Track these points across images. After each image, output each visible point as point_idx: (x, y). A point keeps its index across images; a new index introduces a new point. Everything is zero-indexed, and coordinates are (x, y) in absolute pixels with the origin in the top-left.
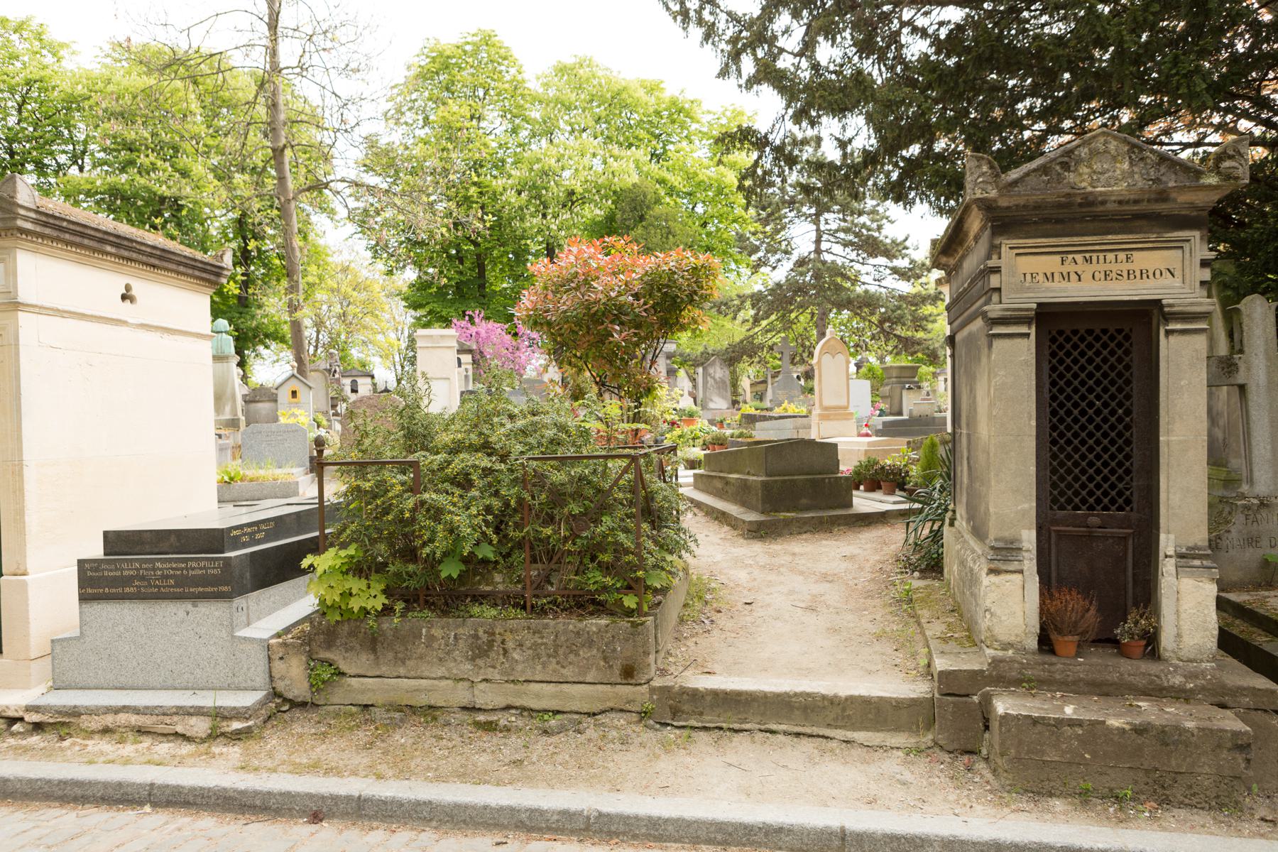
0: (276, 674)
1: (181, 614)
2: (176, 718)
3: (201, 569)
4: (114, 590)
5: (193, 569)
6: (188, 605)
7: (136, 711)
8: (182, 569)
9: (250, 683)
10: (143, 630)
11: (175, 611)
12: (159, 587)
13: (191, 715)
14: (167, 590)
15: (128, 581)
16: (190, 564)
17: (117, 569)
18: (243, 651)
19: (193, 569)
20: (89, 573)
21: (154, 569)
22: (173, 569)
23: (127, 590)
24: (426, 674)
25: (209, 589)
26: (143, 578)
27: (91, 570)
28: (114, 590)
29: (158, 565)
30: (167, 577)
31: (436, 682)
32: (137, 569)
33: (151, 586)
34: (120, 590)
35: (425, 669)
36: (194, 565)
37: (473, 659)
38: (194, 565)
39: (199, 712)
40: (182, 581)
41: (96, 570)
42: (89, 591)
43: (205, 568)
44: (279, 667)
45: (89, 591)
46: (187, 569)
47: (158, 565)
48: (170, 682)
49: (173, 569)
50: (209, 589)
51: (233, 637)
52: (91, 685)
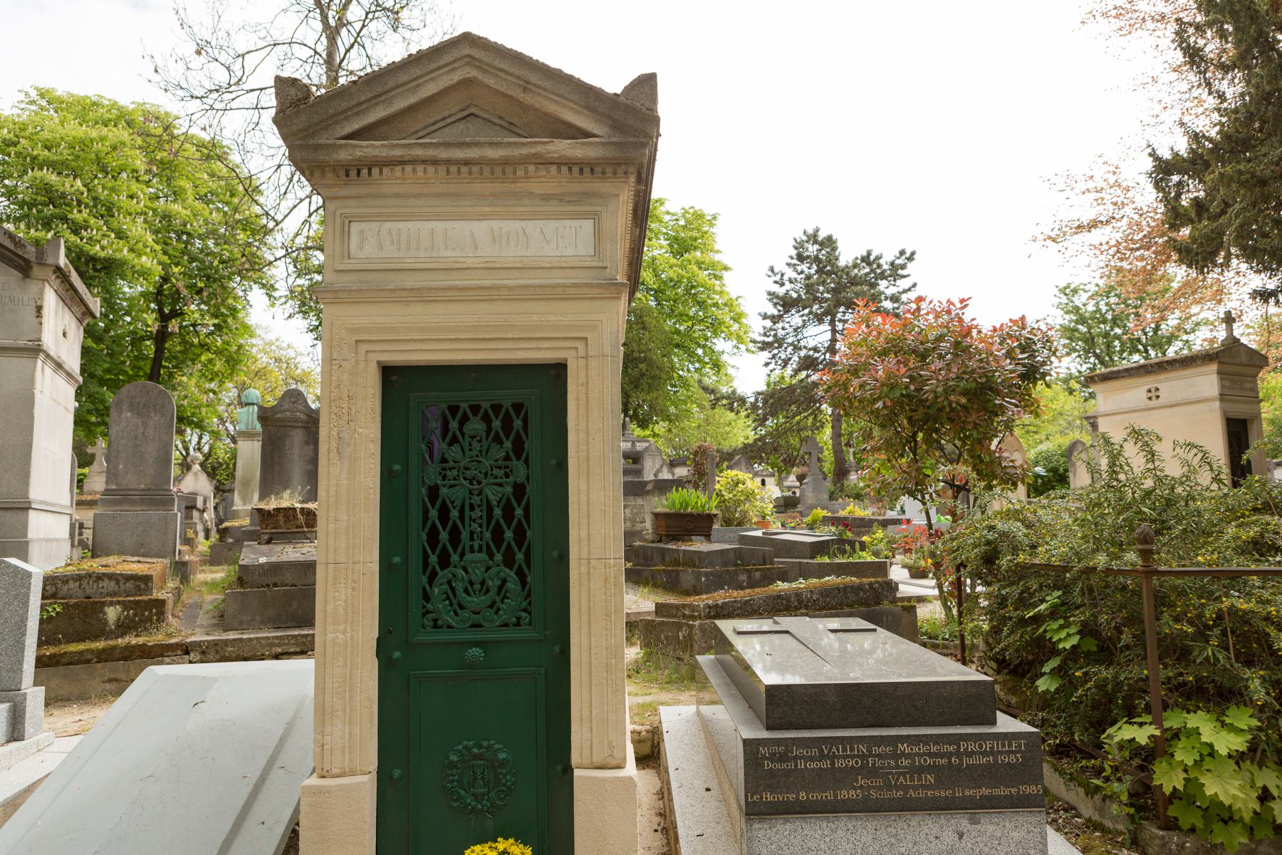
1: (949, 837)
3: (985, 754)
4: (816, 796)
5: (970, 754)
6: (963, 822)
8: (949, 755)
11: (935, 831)
12: (906, 788)
14: (921, 794)
17: (822, 757)
19: (970, 754)
20: (768, 765)
21: (896, 756)
22: (931, 755)
23: (844, 794)
25: (1002, 791)
26: (873, 772)
27: (772, 758)
29: (904, 747)
30: (921, 770)
32: (863, 757)
33: (889, 786)
36: (972, 747)
38: (972, 747)
41: (783, 758)
42: (768, 797)
43: (992, 752)
45: (768, 797)
47: (904, 747)
49: (931, 755)
50: (1002, 791)
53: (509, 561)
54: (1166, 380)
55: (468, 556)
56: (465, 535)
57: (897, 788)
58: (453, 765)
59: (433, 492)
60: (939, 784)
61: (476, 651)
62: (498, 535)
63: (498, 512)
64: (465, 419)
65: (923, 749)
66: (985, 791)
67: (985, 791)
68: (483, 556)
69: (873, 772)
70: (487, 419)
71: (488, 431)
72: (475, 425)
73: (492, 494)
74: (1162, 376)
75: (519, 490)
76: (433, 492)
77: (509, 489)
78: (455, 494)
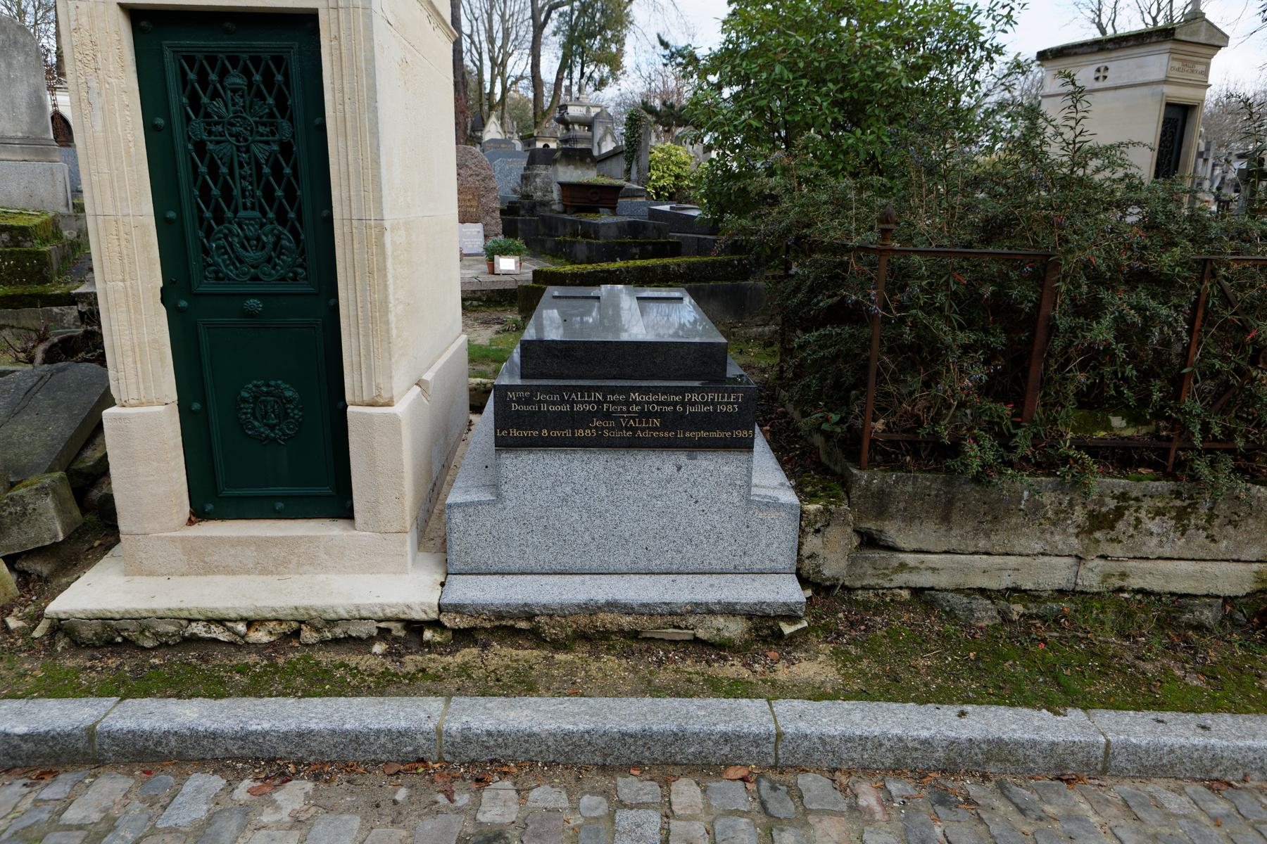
0: (806, 551)
1: (669, 468)
2: (692, 620)
3: (706, 404)
4: (557, 433)
5: (693, 404)
6: (682, 458)
7: (627, 609)
8: (675, 404)
9: (768, 565)
10: (603, 491)
11: (658, 464)
12: (634, 430)
13: (711, 612)
14: (647, 434)
15: (582, 420)
16: (687, 397)
17: (563, 402)
18: (762, 521)
19: (693, 404)
21: (628, 403)
22: (658, 403)
24: (1017, 549)
25: (718, 434)
26: (608, 416)
27: (519, 401)
28: (557, 433)
29: (635, 396)
31: (1028, 560)
32: (598, 403)
33: (621, 429)
34: (568, 433)
35: (1020, 544)
36: (695, 397)
37: (1091, 532)
38: (695, 397)
39: (730, 610)
40: (674, 421)
41: (528, 401)
42: (515, 433)
43: (712, 403)
44: (813, 543)
46: (683, 403)
47: (635, 396)
48: (642, 565)
49: (658, 403)
50: (718, 434)
51: (749, 502)
52: (514, 568)
53: (282, 218)
54: (1118, 58)
55: (242, 213)
56: (236, 192)
57: (627, 429)
58: (245, 400)
59: (200, 147)
60: (664, 428)
61: (253, 303)
62: (268, 192)
63: (266, 170)
64: (223, 73)
65: (652, 398)
66: (703, 434)
67: (703, 434)
68: (257, 214)
69: (608, 416)
70: (247, 73)
71: (250, 85)
72: (236, 79)
73: (260, 152)
74: (1114, 54)
75: (286, 149)
76: (200, 147)
77: (275, 148)
78: (222, 150)
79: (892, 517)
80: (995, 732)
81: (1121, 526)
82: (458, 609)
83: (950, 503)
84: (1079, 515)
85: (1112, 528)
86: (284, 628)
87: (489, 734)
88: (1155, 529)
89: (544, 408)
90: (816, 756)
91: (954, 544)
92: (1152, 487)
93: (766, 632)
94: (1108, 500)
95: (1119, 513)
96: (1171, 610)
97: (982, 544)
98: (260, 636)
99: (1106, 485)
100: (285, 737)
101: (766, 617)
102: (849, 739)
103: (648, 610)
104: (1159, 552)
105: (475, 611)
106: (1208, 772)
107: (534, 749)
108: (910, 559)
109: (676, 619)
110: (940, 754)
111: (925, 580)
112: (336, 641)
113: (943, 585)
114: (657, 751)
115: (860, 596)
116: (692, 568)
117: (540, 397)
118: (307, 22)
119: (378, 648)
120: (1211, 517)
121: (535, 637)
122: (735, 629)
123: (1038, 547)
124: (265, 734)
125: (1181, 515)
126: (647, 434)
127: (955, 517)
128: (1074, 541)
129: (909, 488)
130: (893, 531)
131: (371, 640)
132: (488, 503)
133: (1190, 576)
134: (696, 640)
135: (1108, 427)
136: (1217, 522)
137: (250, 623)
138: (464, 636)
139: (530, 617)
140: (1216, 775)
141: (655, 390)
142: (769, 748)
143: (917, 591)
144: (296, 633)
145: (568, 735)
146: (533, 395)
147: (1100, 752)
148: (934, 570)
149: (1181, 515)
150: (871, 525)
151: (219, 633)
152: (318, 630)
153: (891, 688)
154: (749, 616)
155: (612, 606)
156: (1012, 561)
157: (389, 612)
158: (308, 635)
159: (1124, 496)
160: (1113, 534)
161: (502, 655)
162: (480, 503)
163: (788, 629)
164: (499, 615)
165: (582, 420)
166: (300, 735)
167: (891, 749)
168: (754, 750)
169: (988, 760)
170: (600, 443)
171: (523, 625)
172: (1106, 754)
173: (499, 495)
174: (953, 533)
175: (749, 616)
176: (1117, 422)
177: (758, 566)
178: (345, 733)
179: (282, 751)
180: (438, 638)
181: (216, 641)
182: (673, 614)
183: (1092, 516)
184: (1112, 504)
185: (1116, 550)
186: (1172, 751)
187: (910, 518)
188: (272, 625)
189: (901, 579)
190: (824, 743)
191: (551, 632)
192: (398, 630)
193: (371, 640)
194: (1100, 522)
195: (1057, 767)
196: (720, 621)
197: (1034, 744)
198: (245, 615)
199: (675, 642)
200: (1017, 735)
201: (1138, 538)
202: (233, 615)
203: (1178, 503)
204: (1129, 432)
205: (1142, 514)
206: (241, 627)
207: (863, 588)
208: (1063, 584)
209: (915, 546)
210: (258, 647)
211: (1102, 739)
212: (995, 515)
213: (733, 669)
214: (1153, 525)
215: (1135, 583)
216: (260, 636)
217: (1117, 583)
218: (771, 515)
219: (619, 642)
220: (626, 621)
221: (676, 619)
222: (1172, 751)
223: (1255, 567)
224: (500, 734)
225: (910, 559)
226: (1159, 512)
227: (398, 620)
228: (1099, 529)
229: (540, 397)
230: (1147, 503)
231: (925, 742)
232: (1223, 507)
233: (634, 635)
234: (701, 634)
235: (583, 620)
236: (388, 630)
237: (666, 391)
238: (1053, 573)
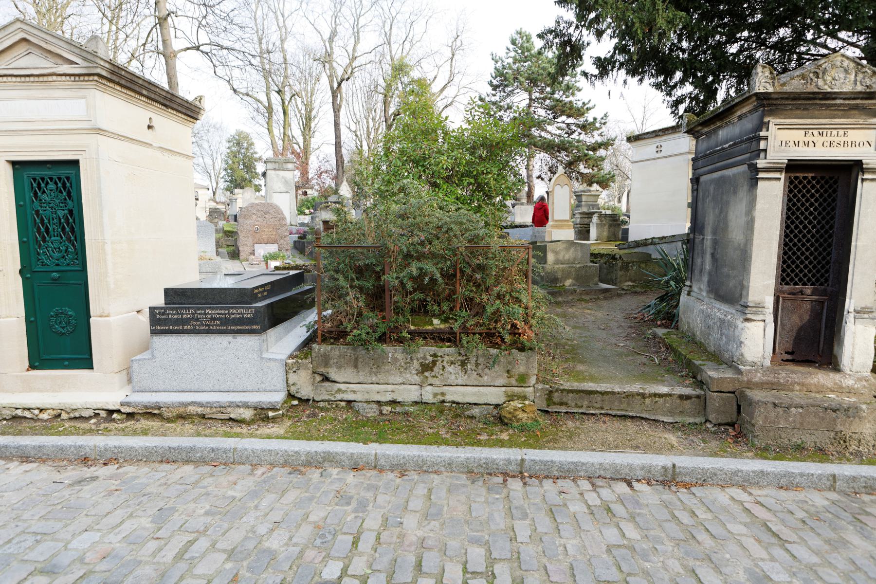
0: (290, 382)
2: (229, 410)
4: (176, 328)
5: (233, 314)
6: (230, 338)
7: (201, 405)
8: (225, 314)
9: (273, 388)
10: (197, 353)
13: (238, 406)
14: (215, 328)
15: (185, 322)
16: (231, 311)
17: (178, 314)
18: (268, 367)
19: (233, 314)
20: (158, 316)
21: (205, 314)
23: (186, 327)
24: (391, 381)
25: (245, 327)
26: (197, 320)
27: (159, 314)
28: (176, 328)
29: (208, 311)
30: (215, 319)
31: (397, 387)
32: (193, 314)
34: (181, 327)
35: (392, 379)
36: (234, 311)
37: (423, 372)
38: (234, 311)
39: (246, 406)
40: (225, 322)
41: (163, 314)
42: (158, 328)
43: (242, 313)
44: (293, 378)
45: (158, 328)
46: (229, 314)
48: (217, 388)
50: (245, 327)
51: (262, 358)
52: (160, 389)
53: (69, 240)
54: (666, 140)
55: (53, 238)
56: (51, 229)
57: (206, 325)
58: (52, 316)
59: (37, 212)
60: (221, 325)
61: (54, 274)
62: (63, 229)
63: (63, 220)
64: (47, 183)
65: (216, 312)
66: (239, 327)
67: (239, 327)
68: (59, 238)
69: (197, 320)
70: (56, 183)
71: (57, 188)
72: (52, 186)
73: (60, 213)
74: (664, 138)
75: (71, 212)
76: (37, 212)
77: (66, 212)
78: (46, 214)
79: (331, 367)
80: (328, 449)
81: (436, 369)
82: (128, 404)
83: (356, 359)
84: (416, 364)
85: (432, 371)
86: (55, 412)
87: (115, 447)
88: (452, 371)
89: (170, 316)
90: (251, 458)
91: (361, 379)
92: (447, 351)
93: (263, 416)
94: (428, 357)
95: (434, 363)
96: (459, 410)
97: (374, 379)
98: (44, 416)
99: (426, 351)
100: (34, 447)
101: (263, 409)
102: (264, 451)
103: (209, 405)
104: (456, 382)
105: (135, 405)
106: (421, 467)
107: (133, 454)
108: (343, 387)
109: (222, 410)
110: (303, 458)
111: (351, 397)
112: (75, 418)
113: (359, 399)
114: (184, 455)
115: (321, 404)
116: (239, 389)
117: (168, 312)
118: (75, 164)
119: (93, 421)
120: (477, 365)
121: (160, 416)
122: (248, 414)
123: (400, 380)
124: (26, 446)
125: (463, 364)
126: (215, 328)
127: (360, 365)
128: (415, 377)
129: (337, 353)
130: (333, 374)
131: (90, 418)
132: (149, 359)
133: (474, 394)
134: (231, 419)
135: (432, 324)
136: (480, 367)
137: (41, 410)
138: (130, 416)
139: (160, 408)
140: (425, 468)
141: (217, 308)
142: (231, 455)
143: (349, 402)
144: (60, 415)
145: (147, 448)
146: (165, 311)
147: (373, 458)
148: (354, 392)
149: (463, 364)
150: (322, 370)
151: (27, 414)
152: (68, 413)
153: (307, 436)
154: (255, 409)
155: (193, 403)
156: (390, 387)
157: (99, 406)
158: (64, 416)
159: (435, 355)
160: (433, 374)
161: (144, 423)
162: (145, 359)
163: (271, 414)
164: (146, 407)
165: (185, 322)
166: (40, 447)
167: (282, 456)
168: (225, 456)
169: (324, 461)
170: (195, 332)
171: (156, 412)
172: (376, 459)
173: (153, 356)
174: (360, 373)
175: (255, 409)
176: (436, 321)
177: (269, 389)
178: (57, 446)
179: (32, 454)
180: (119, 417)
181: (25, 418)
182: (221, 407)
183: (422, 365)
184: (431, 359)
185: (436, 381)
186: (404, 458)
187: (340, 367)
188: (49, 411)
189: (339, 396)
190: (254, 453)
191: (166, 414)
192: (103, 414)
193: (90, 418)
194: (426, 368)
195: (355, 464)
196: (241, 410)
197: (344, 454)
198: (39, 406)
199: (222, 420)
200: (336, 450)
201: (446, 375)
202: (33, 407)
203: (460, 358)
204: (442, 326)
205: (445, 364)
206: (37, 412)
207: (322, 401)
208: (417, 399)
209: (344, 380)
210: (42, 420)
211: (374, 452)
212: (378, 364)
213: (244, 430)
214: (451, 369)
215: (449, 398)
216: (44, 416)
217: (441, 398)
218: (272, 364)
219: (197, 420)
220: (200, 410)
221: (222, 410)
222: (404, 458)
223: (503, 389)
224: (120, 447)
225: (343, 387)
226: (452, 363)
227: (103, 410)
228: (427, 371)
229: (168, 312)
230: (446, 358)
231: (296, 452)
232: (481, 360)
233: (203, 417)
234: (232, 416)
235: (182, 410)
236: (99, 414)
237: (221, 308)
238: (409, 393)
